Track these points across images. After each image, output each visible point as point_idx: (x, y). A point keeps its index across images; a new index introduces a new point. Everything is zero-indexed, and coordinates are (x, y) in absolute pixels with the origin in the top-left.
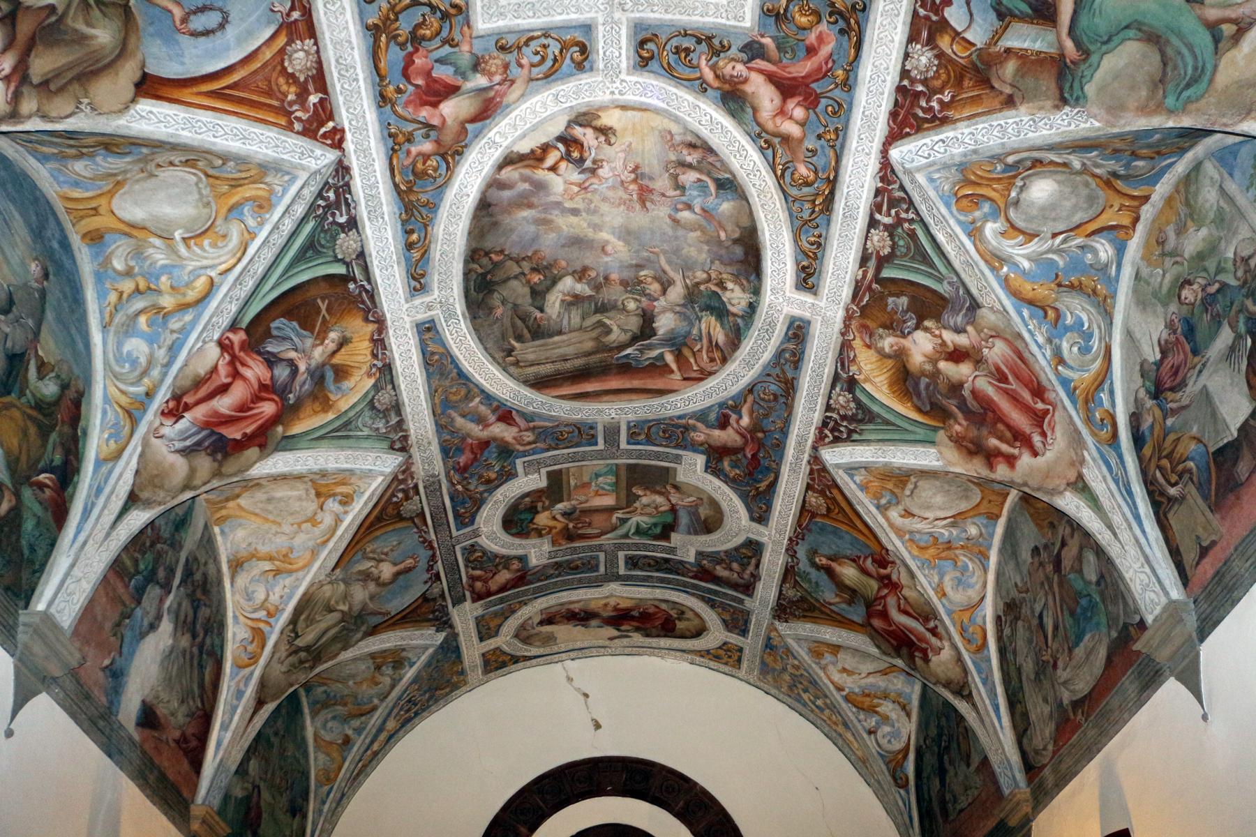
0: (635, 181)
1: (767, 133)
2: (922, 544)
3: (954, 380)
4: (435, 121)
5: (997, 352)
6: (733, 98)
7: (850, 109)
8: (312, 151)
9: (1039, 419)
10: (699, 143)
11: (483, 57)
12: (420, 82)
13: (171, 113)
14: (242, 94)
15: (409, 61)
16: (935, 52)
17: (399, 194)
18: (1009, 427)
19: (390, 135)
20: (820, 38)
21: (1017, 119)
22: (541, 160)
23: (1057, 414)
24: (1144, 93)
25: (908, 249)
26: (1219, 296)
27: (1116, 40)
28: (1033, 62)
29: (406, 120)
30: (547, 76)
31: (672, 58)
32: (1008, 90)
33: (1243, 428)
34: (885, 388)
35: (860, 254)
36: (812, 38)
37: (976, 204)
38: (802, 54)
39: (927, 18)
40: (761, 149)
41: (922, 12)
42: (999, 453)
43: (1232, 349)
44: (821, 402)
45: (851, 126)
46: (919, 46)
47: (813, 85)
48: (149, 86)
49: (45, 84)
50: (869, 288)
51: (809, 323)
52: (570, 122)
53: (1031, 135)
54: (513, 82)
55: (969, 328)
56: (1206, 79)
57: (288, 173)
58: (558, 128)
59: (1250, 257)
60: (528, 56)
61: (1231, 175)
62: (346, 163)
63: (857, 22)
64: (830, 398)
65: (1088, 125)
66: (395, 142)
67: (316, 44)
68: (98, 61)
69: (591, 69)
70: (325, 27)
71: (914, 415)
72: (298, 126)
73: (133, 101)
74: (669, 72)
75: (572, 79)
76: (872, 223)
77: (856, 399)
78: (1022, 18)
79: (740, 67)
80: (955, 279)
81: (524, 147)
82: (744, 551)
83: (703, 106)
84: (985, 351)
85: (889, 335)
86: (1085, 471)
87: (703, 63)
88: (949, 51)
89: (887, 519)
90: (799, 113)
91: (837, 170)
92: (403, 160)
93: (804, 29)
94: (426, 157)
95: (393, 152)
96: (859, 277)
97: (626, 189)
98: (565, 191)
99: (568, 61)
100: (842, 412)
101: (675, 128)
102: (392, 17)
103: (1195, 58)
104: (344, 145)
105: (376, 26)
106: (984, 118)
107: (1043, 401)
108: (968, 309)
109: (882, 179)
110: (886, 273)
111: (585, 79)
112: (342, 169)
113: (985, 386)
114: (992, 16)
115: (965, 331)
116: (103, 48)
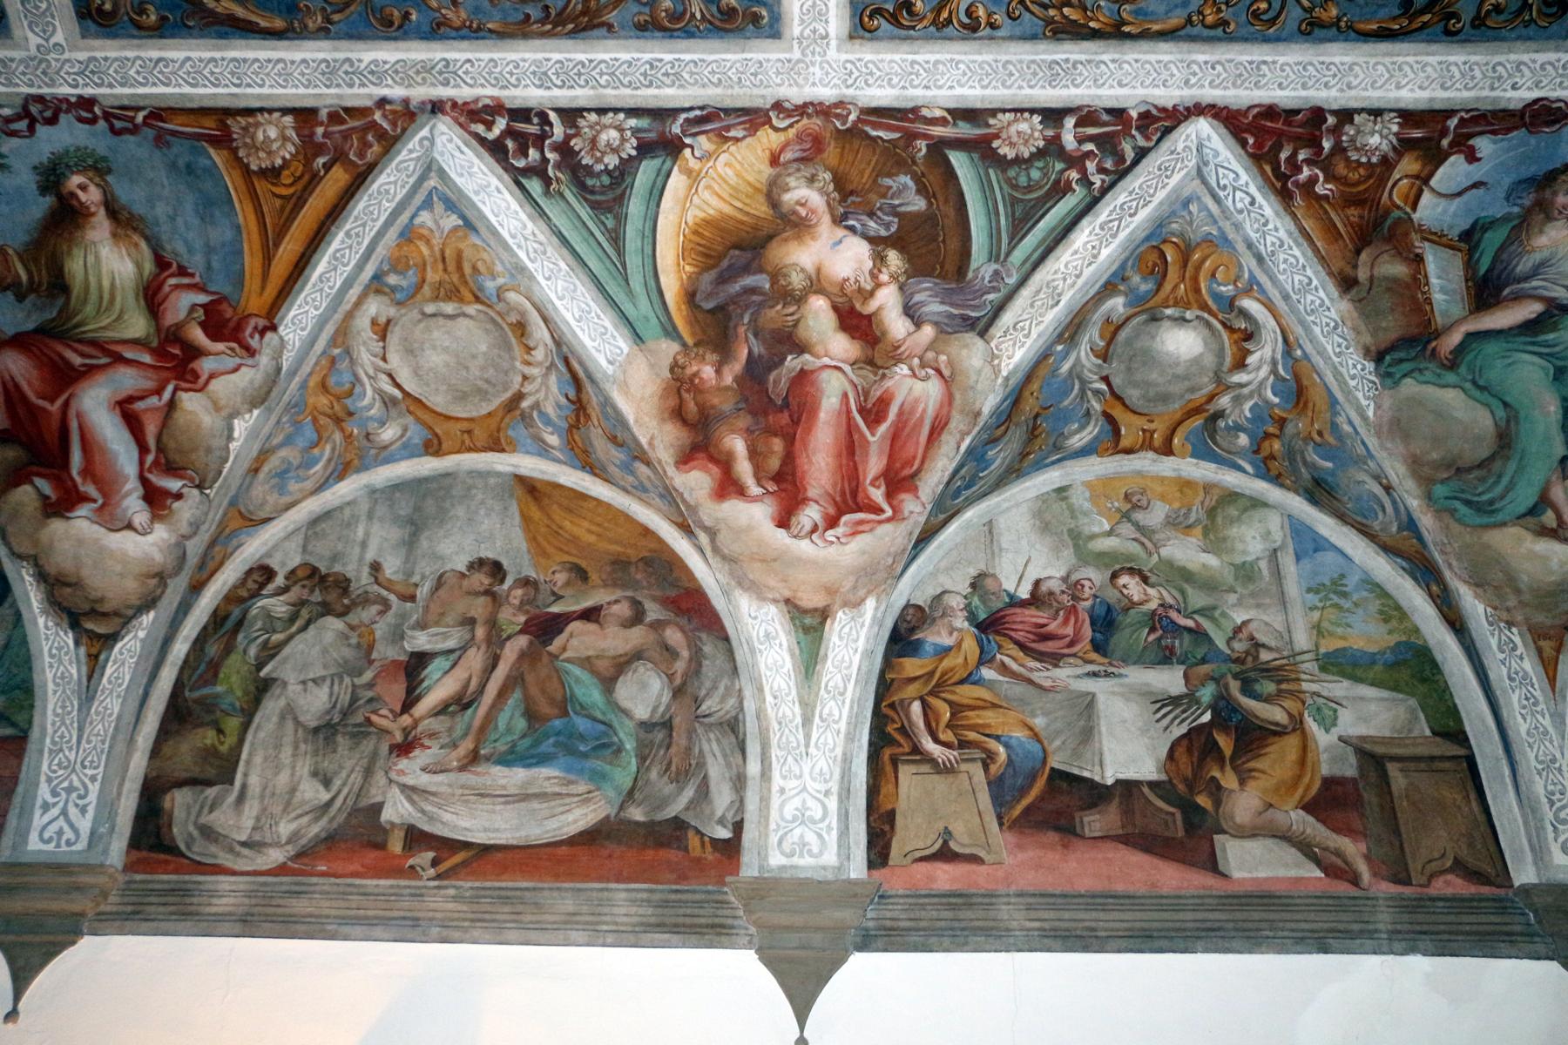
2: (331, 381)
3: (802, 332)
5: (912, 389)
9: (848, 501)
16: (1391, 154)
18: (789, 458)
21: (1327, 302)
23: (888, 527)
24: (1435, 456)
25: (1029, 188)
26: (1186, 635)
27: (1485, 397)
28: (1414, 299)
32: (1362, 274)
33: (1128, 788)
34: (694, 215)
35: (979, 105)
37: (1152, 273)
39: (1444, 132)
41: (1453, 123)
42: (725, 464)
43: (1175, 701)
44: (579, 95)
45: (1237, 47)
46: (1395, 128)
50: (911, 137)
51: (776, 35)
55: (928, 331)
56: (1486, 520)
59: (1263, 646)
61: (1298, 558)
63: (1425, 25)
64: (601, 111)
65: (1364, 403)
71: (671, 285)
76: (1053, 116)
77: (626, 169)
78: (1470, 265)
80: (1012, 281)
84: (903, 369)
85: (821, 191)
86: (841, 616)
88: (1396, 175)
89: (358, 304)
91: (1145, 35)
96: (925, 112)
100: (576, 143)
103: (1502, 497)
106: (1310, 253)
107: (889, 496)
108: (965, 318)
109: (1145, 116)
110: (958, 160)
113: (833, 392)
115: (918, 324)
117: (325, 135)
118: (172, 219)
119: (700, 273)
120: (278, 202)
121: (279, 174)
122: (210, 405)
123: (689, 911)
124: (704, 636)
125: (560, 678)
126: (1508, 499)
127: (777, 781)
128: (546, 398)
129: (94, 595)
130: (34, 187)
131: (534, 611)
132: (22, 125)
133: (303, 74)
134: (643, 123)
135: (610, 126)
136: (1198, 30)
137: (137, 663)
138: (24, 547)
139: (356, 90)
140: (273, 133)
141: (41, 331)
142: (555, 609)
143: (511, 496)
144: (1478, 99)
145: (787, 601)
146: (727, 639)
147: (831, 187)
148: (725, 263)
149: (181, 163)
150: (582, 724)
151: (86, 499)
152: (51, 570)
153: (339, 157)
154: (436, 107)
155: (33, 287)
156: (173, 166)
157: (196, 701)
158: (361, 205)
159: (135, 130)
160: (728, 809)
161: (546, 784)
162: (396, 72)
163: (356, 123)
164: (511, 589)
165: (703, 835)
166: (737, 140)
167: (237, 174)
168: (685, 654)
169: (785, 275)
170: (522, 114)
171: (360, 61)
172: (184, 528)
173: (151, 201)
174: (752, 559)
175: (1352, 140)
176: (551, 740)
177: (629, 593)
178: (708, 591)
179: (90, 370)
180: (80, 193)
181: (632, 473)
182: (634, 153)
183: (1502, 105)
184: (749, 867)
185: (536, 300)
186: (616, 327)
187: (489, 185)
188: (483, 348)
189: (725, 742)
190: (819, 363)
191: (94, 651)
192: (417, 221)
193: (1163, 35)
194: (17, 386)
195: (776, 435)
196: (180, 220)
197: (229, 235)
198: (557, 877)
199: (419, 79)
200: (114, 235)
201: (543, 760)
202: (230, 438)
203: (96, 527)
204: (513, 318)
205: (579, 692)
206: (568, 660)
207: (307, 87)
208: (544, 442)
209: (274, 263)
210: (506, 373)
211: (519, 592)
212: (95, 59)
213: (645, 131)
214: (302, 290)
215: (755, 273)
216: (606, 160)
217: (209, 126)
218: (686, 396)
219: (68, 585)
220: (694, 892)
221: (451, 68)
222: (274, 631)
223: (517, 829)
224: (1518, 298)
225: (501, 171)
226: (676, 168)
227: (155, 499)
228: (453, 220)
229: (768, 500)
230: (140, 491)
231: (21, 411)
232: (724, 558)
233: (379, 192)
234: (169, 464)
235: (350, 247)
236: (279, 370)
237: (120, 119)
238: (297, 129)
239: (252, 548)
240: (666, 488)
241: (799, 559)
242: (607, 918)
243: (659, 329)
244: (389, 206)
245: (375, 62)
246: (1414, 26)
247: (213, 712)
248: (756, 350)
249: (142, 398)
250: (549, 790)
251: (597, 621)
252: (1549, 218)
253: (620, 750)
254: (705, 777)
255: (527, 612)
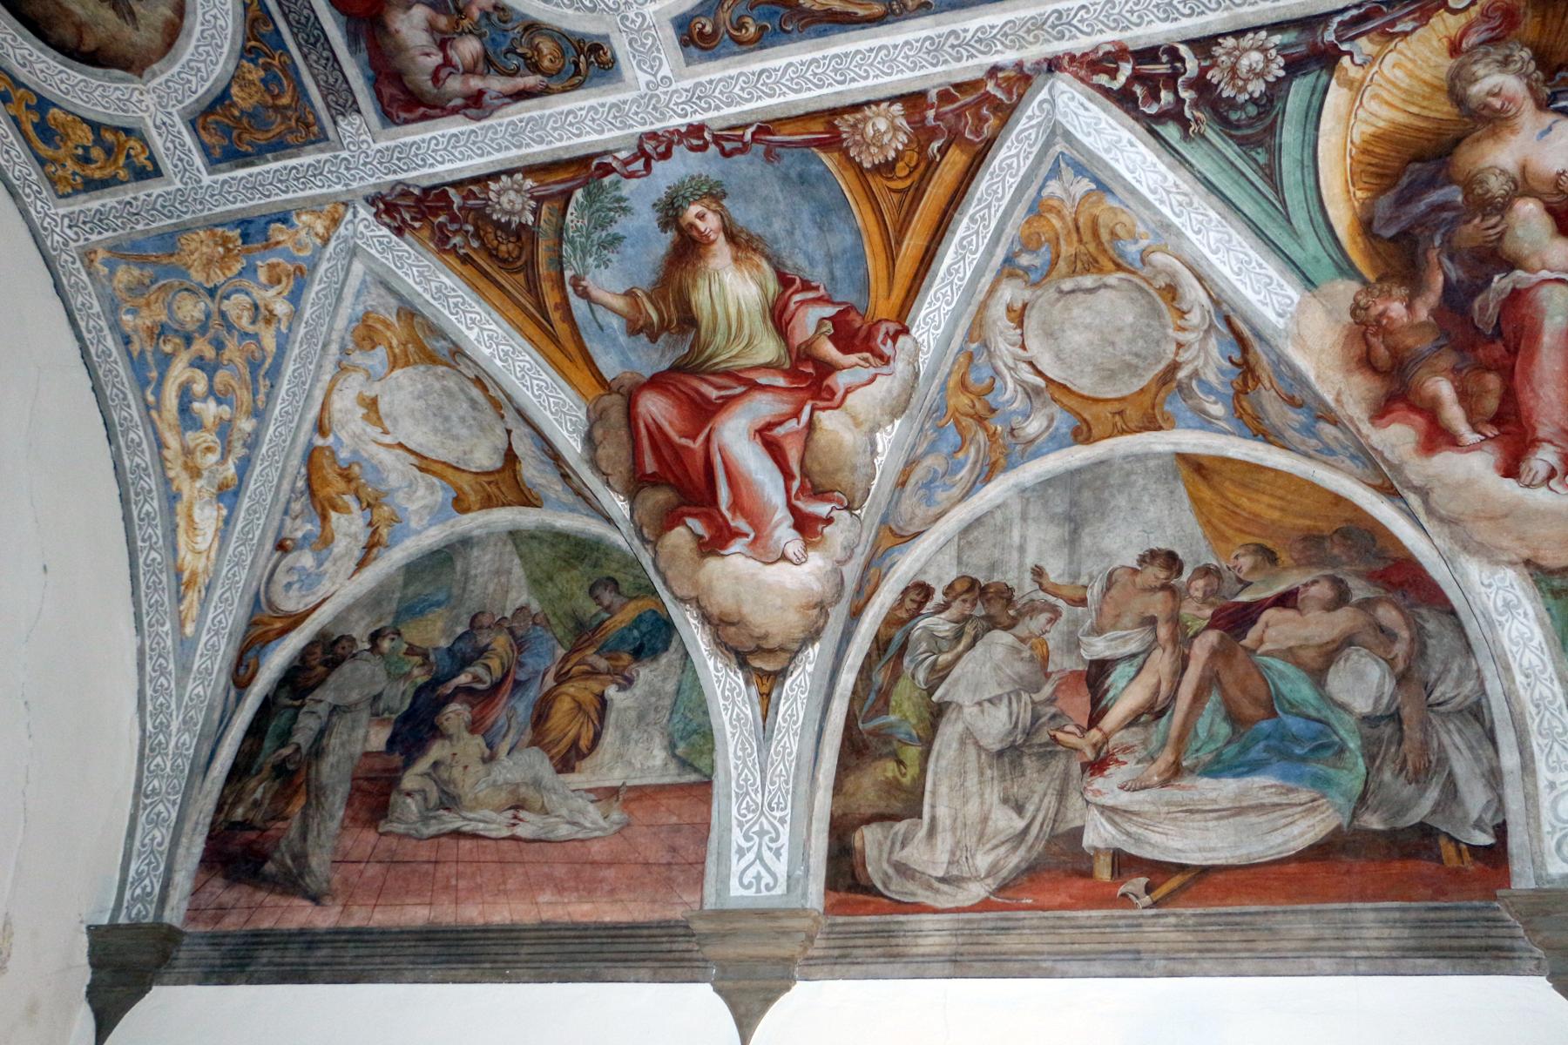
2: (971, 378)
3: (1509, 246)
18: (1509, 396)
42: (1430, 412)
64: (1239, 33)
71: (1342, 217)
82: (546, 47)
85: (1520, 74)
89: (992, 291)
100: (1214, 76)
117: (936, 118)
118: (791, 233)
119: (1375, 197)
120: (896, 197)
121: (893, 168)
122: (849, 421)
123: (1453, 932)
124: (1424, 611)
125: (1260, 674)
127: (1543, 774)
128: (1206, 363)
129: (757, 632)
130: (656, 224)
131: (1220, 602)
132: (638, 165)
133: (907, 57)
134: (1289, 37)
135: (1251, 49)
137: (809, 698)
138: (685, 590)
139: (964, 63)
140: (882, 125)
141: (676, 369)
142: (1244, 598)
143: (1175, 478)
145: (1527, 562)
146: (1453, 612)
147: (1532, 65)
148: (1405, 180)
149: (793, 174)
150: (1294, 724)
151: (738, 534)
152: (714, 611)
153: (954, 138)
154: (1053, 65)
155: (664, 326)
156: (785, 178)
157: (870, 733)
158: (983, 185)
159: (744, 149)
160: (1486, 809)
161: (1262, 794)
162: (1006, 35)
163: (969, 99)
164: (1190, 580)
165: (1457, 842)
166: (1406, 34)
167: (850, 175)
168: (1405, 634)
169: (1481, 182)
170: (1149, 54)
171: (965, 31)
172: (840, 554)
173: (767, 219)
174: (1477, 518)
176: (1262, 745)
177: (1329, 572)
178: (1420, 559)
179: (727, 401)
180: (698, 223)
181: (1315, 435)
182: (1282, 73)
184: (1523, 878)
185: (1188, 258)
186: (1281, 273)
187: (1120, 141)
188: (1130, 319)
189: (1468, 733)
190: (1535, 278)
191: (765, 690)
192: (1045, 193)
194: (659, 428)
195: (1489, 370)
196: (798, 233)
197: (849, 239)
198: (1290, 898)
199: (1031, 38)
200: (736, 260)
201: (1254, 768)
202: (874, 453)
203: (751, 562)
204: (1161, 282)
205: (1285, 688)
206: (1267, 654)
207: (912, 70)
208: (1208, 415)
209: (898, 263)
210: (1158, 343)
211: (1200, 583)
212: (700, 84)
213: (1292, 46)
214: (930, 286)
215: (1443, 186)
216: (1250, 88)
217: (818, 129)
218: (1373, 340)
219: (732, 624)
220: (1457, 908)
221: (1064, 20)
222: (941, 652)
223: (1237, 847)
225: (1132, 122)
226: (1333, 82)
227: (805, 525)
228: (1085, 185)
229: (1489, 447)
230: (790, 520)
231: (666, 453)
232: (1442, 520)
233: (1001, 169)
234: (815, 489)
235: (977, 233)
236: (917, 375)
237: (729, 141)
238: (907, 116)
239: (906, 566)
240: (1361, 448)
241: (1537, 511)
242: (1357, 943)
243: (1333, 270)
244: (1013, 182)
245: (981, 29)
247: (890, 743)
248: (1453, 276)
249: (780, 423)
250: (1266, 801)
251: (1294, 607)
253: (1342, 750)
254: (1450, 774)
255: (1212, 604)
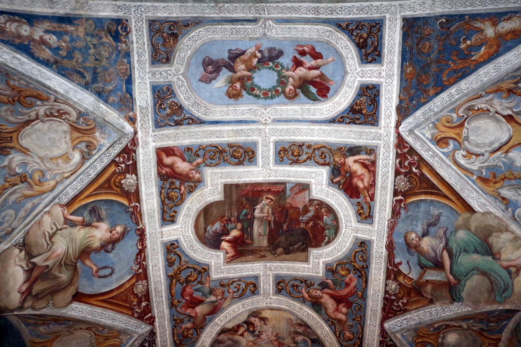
0: (276, 340)
1: (331, 318)
4: (193, 315)
6: (316, 305)
7: (365, 308)
8: (141, 326)
10: (303, 324)
11: (214, 289)
12: (188, 298)
13: (85, 308)
14: (115, 301)
15: (184, 290)
17: (176, 345)
19: (174, 320)
20: (351, 279)
22: (237, 331)
24: (486, 295)
27: (470, 275)
28: (439, 285)
29: (181, 314)
30: (240, 297)
31: (291, 289)
32: (430, 297)
36: (347, 279)
38: (344, 286)
39: (393, 270)
40: (330, 326)
45: (367, 315)
46: (391, 281)
47: (349, 298)
48: (79, 297)
49: (37, 295)
52: (249, 315)
53: (442, 315)
54: (226, 299)
56: (510, 289)
57: (129, 335)
58: (244, 318)
60: (232, 289)
62: (154, 331)
65: (466, 310)
66: (176, 323)
67: (147, 282)
68: (60, 286)
69: (258, 294)
70: (151, 276)
72: (136, 315)
73: (71, 303)
74: (290, 295)
75: (250, 298)
78: (430, 268)
79: (319, 292)
81: (230, 326)
83: (304, 308)
87: (304, 291)
90: (344, 310)
92: (179, 330)
93: (344, 276)
94: (188, 329)
95: (174, 328)
97: (273, 343)
98: (247, 344)
99: (248, 291)
101: (293, 317)
102: (178, 272)
103: (503, 280)
104: (154, 324)
105: (172, 276)
109: (382, 337)
111: (255, 298)
112: (152, 333)
114: (418, 268)
116: (63, 281)
126: (504, 279)
136: (362, 322)
144: (385, 261)
175: (393, 291)
183: (387, 256)
193: (363, 329)
224: (442, 257)
246: (364, 275)
252: (419, 246)
